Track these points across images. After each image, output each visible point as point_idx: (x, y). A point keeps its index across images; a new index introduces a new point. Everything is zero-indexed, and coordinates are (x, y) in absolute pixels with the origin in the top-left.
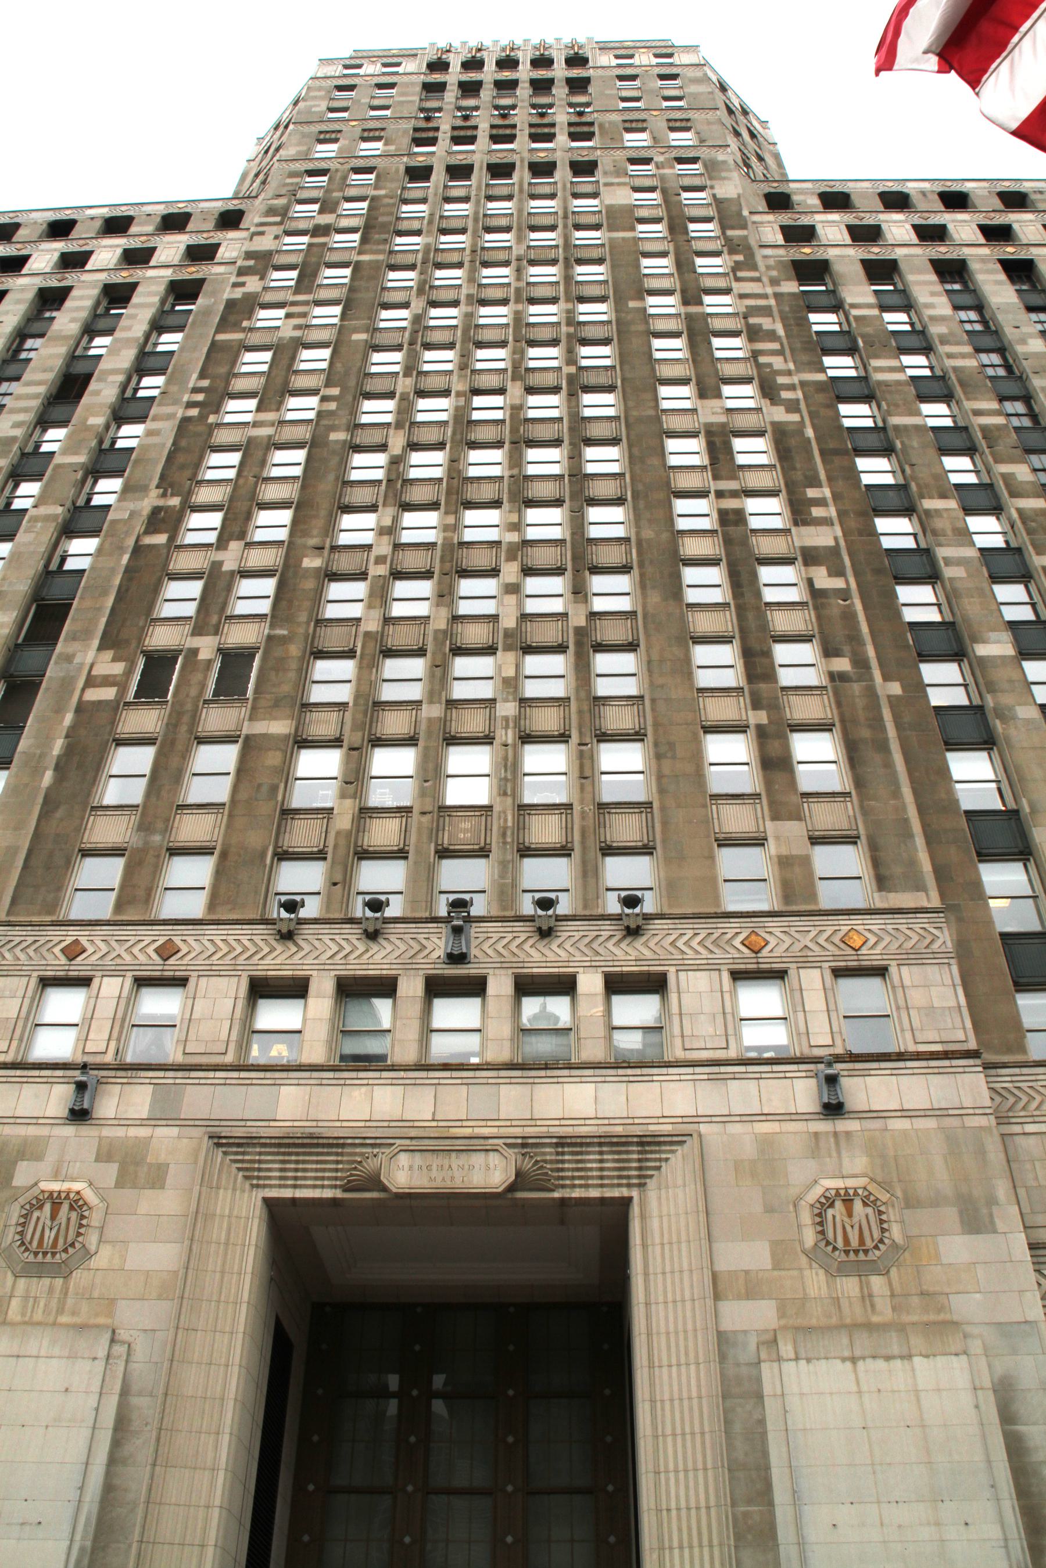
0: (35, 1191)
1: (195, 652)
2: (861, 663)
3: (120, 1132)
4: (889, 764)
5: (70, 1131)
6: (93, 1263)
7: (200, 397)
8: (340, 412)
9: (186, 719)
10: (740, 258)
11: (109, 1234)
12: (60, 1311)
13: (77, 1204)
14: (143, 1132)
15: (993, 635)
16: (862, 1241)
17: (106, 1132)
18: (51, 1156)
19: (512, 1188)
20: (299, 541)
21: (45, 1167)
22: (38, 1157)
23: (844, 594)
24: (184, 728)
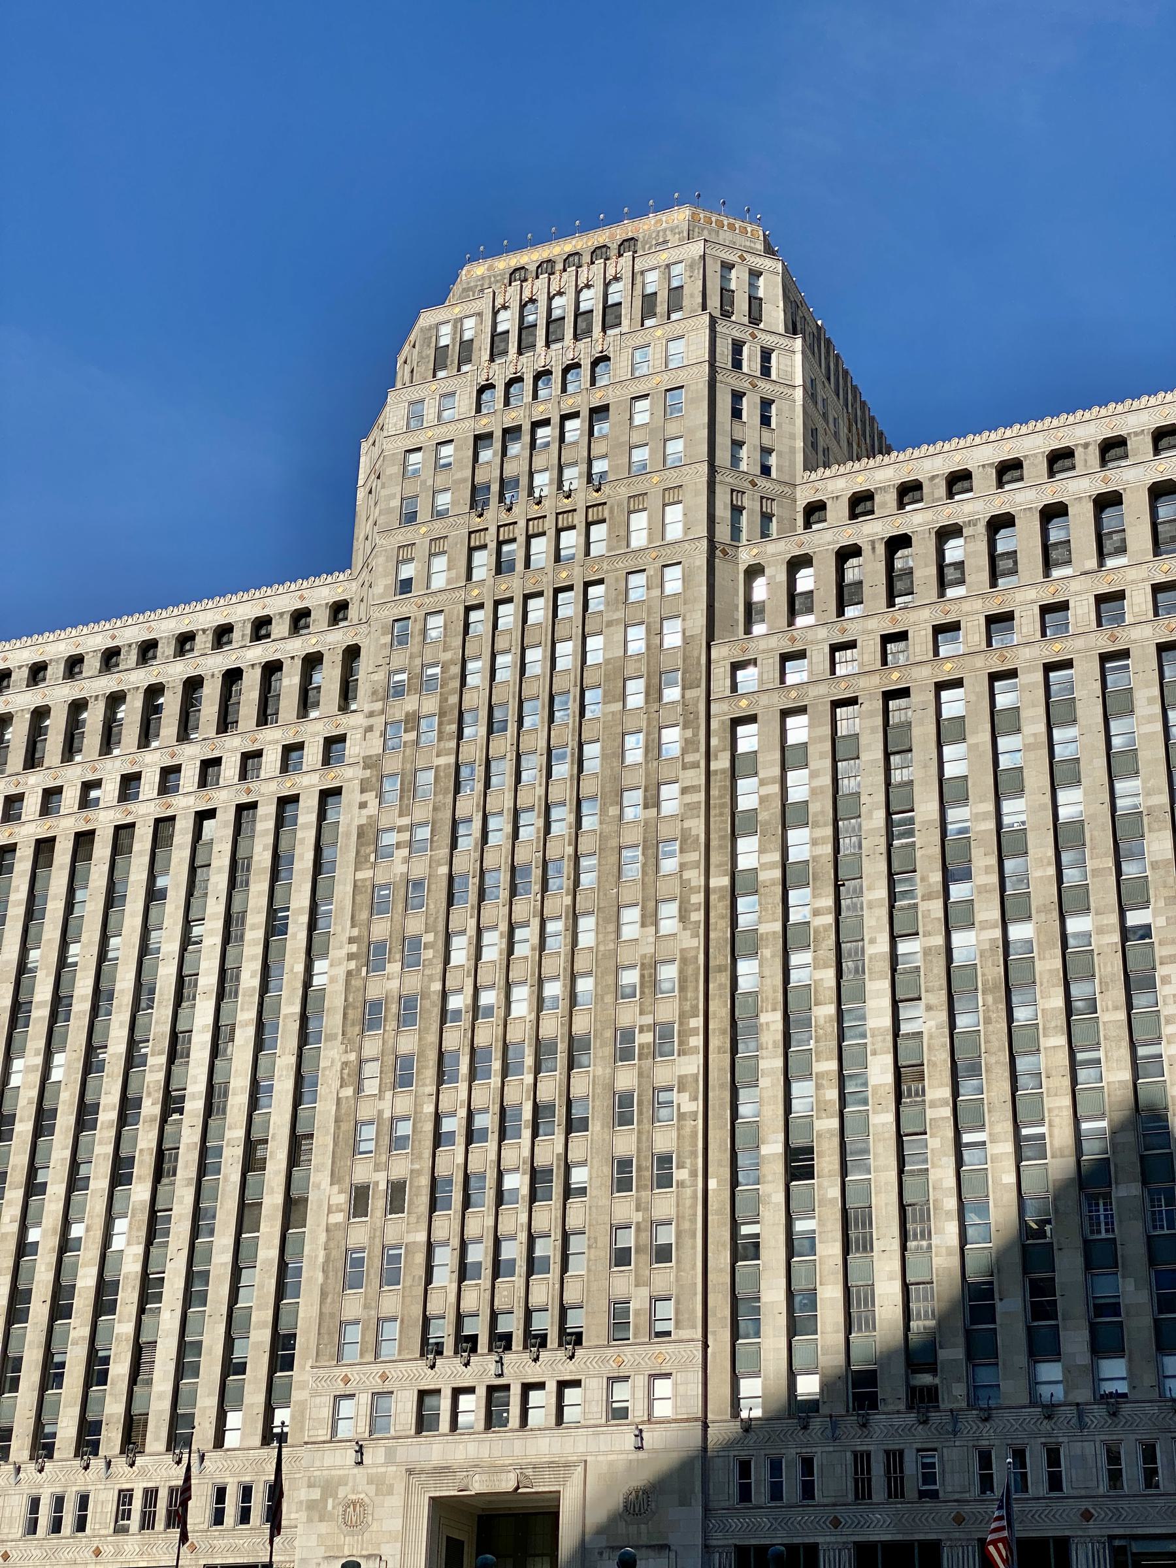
0: (346, 1500)
1: (377, 1184)
3: (374, 1470)
4: (694, 1247)
5: (356, 1470)
6: (370, 1529)
7: (354, 948)
8: (435, 961)
9: (378, 1233)
10: (689, 733)
11: (375, 1517)
12: (362, 1550)
13: (362, 1504)
14: (383, 1470)
15: (772, 1137)
16: (640, 1510)
17: (370, 1471)
18: (350, 1484)
19: (518, 1488)
20: (421, 1090)
21: (348, 1488)
22: (346, 1484)
24: (378, 1241)
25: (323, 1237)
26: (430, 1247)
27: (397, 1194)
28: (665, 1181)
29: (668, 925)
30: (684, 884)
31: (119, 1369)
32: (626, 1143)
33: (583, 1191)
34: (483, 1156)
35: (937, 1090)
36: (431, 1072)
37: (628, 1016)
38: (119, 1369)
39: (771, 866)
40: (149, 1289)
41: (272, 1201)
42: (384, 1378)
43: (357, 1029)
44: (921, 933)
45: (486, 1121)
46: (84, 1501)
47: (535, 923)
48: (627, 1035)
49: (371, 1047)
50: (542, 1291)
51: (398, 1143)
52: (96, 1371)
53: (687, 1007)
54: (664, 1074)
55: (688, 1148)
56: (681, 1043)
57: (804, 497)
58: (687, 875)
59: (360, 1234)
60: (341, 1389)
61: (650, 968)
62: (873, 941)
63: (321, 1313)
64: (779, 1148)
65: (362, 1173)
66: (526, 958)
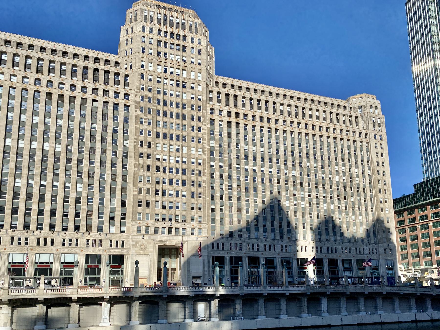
1: (144, 188)
2: (206, 197)
23: (206, 187)
25: (132, 197)
26: (156, 201)
27: (148, 191)
28: (200, 197)
29: (201, 153)
30: (203, 146)
31: (83, 215)
32: (193, 189)
33: (184, 196)
34: (167, 187)
35: (243, 190)
36: (155, 169)
37: (193, 167)
38: (83, 215)
39: (218, 147)
40: (90, 200)
41: (119, 187)
42: (147, 224)
43: (138, 157)
44: (241, 164)
45: (167, 181)
46: (77, 241)
47: (175, 146)
48: (193, 171)
49: (141, 161)
50: (178, 212)
51: (148, 181)
52: (77, 215)
53: (204, 168)
54: (200, 179)
55: (204, 192)
56: (203, 174)
57: (215, 80)
58: (204, 145)
59: (140, 197)
60: (138, 225)
61: (197, 159)
62: (234, 164)
63: (133, 211)
64: (219, 195)
65: (140, 185)
66: (173, 152)
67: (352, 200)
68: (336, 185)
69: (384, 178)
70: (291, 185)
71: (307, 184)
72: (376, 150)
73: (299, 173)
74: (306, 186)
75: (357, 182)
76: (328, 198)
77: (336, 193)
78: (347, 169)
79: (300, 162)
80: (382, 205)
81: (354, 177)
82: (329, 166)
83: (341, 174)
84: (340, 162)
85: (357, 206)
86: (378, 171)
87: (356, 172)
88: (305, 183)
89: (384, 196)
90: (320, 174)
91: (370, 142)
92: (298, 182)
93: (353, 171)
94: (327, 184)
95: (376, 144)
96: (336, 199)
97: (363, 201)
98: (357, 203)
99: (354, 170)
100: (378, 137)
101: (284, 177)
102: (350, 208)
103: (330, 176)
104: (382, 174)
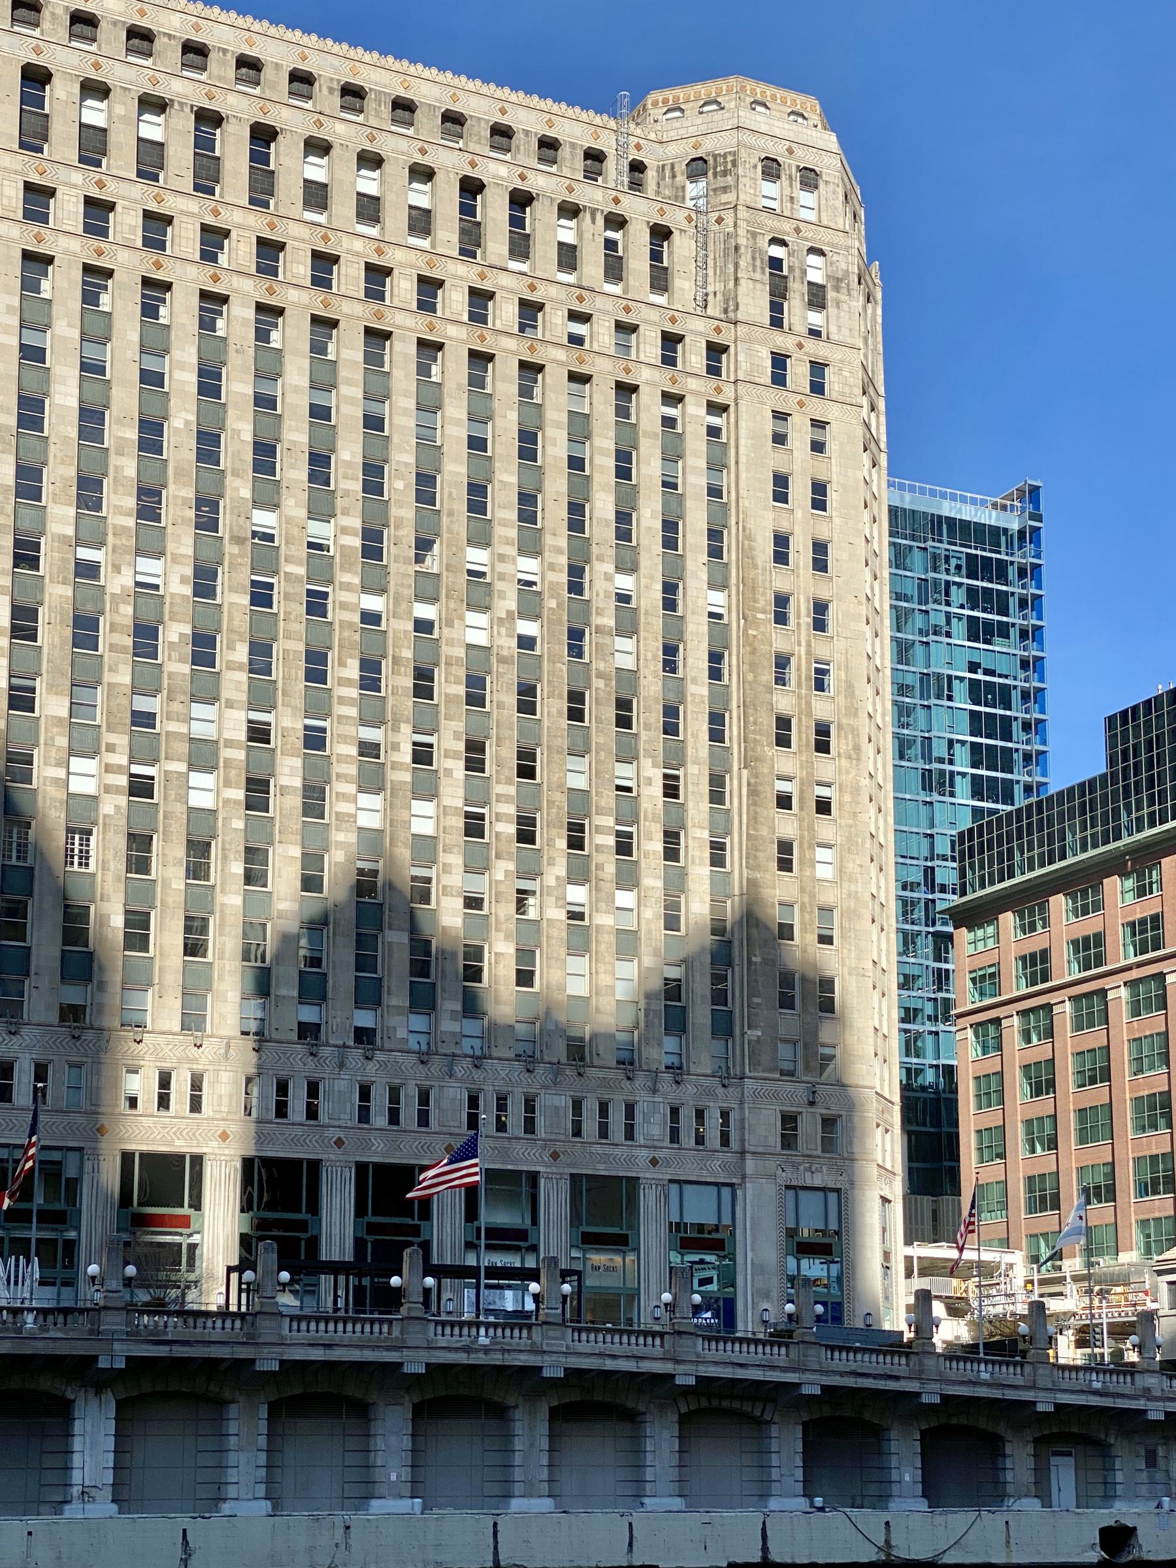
67: (578, 782)
68: (462, 673)
69: (822, 649)
70: (123, 650)
71: (241, 653)
72: (775, 460)
73: (189, 571)
74: (231, 666)
75: (628, 662)
76: (395, 757)
77: (459, 726)
78: (552, 567)
79: (200, 502)
80: (786, 825)
81: (599, 630)
82: (423, 546)
83: (508, 601)
84: (504, 523)
85: (609, 821)
86: (782, 601)
87: (623, 598)
88: (232, 647)
89: (809, 766)
90: (347, 587)
91: (736, 399)
92: (174, 638)
93: (600, 585)
94: (396, 660)
95: (780, 416)
96: (458, 767)
97: (657, 789)
98: (608, 798)
99: (608, 578)
100: (799, 374)
101: (69, 592)
102: (554, 832)
103: (425, 611)
104: (807, 620)
